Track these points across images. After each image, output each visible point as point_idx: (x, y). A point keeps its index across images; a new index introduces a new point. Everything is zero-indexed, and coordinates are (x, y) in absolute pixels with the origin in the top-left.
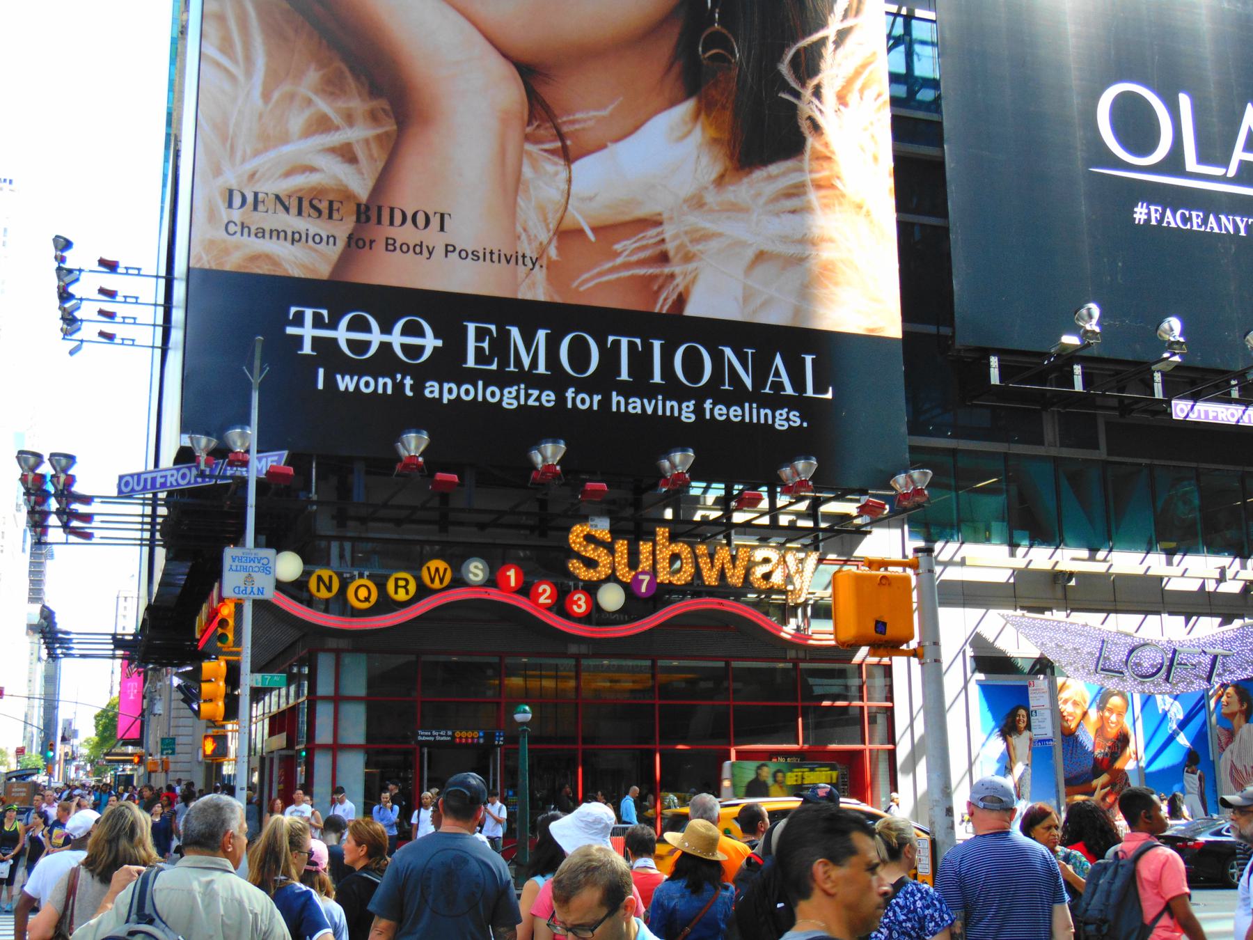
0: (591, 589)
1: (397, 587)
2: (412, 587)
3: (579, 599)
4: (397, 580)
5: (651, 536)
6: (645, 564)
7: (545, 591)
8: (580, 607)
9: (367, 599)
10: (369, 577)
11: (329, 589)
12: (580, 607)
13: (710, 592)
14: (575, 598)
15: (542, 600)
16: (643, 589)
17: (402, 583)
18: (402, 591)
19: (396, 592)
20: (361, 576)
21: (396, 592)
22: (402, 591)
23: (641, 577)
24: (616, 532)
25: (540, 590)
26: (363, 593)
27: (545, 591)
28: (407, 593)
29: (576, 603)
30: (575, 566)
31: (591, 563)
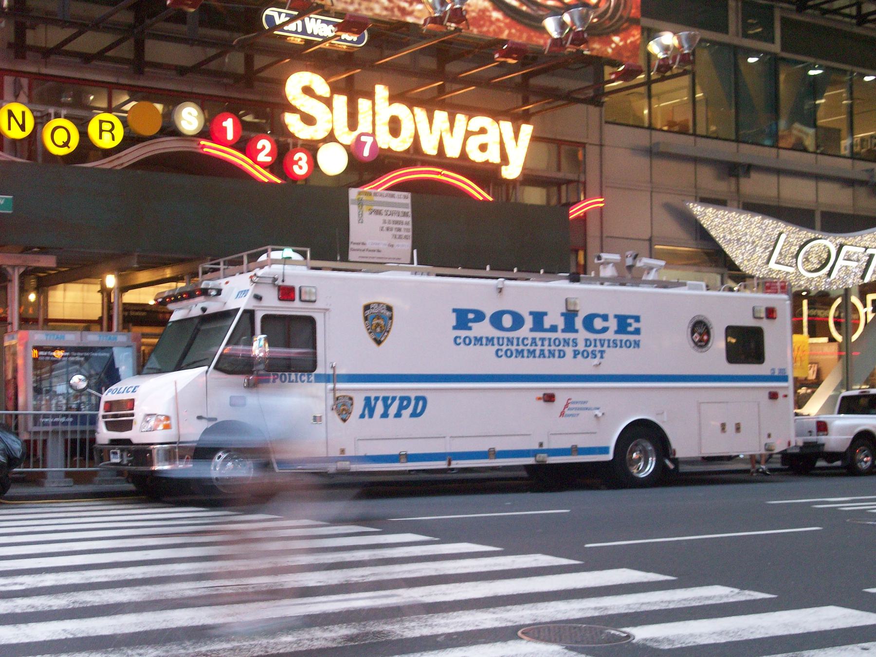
0: (312, 148)
1: (101, 131)
2: (119, 133)
3: (300, 159)
4: (101, 122)
5: (370, 95)
6: (364, 124)
7: (264, 148)
8: (301, 168)
9: (66, 144)
10: (66, 117)
11: (23, 127)
12: (301, 168)
13: (427, 161)
14: (296, 158)
15: (262, 157)
16: (366, 153)
17: (106, 126)
18: (107, 136)
19: (101, 137)
20: (57, 116)
21: (101, 137)
22: (107, 136)
23: (363, 139)
24: (335, 89)
25: (259, 146)
26: (61, 136)
27: (264, 148)
28: (113, 139)
29: (296, 163)
30: (292, 121)
31: (309, 120)
